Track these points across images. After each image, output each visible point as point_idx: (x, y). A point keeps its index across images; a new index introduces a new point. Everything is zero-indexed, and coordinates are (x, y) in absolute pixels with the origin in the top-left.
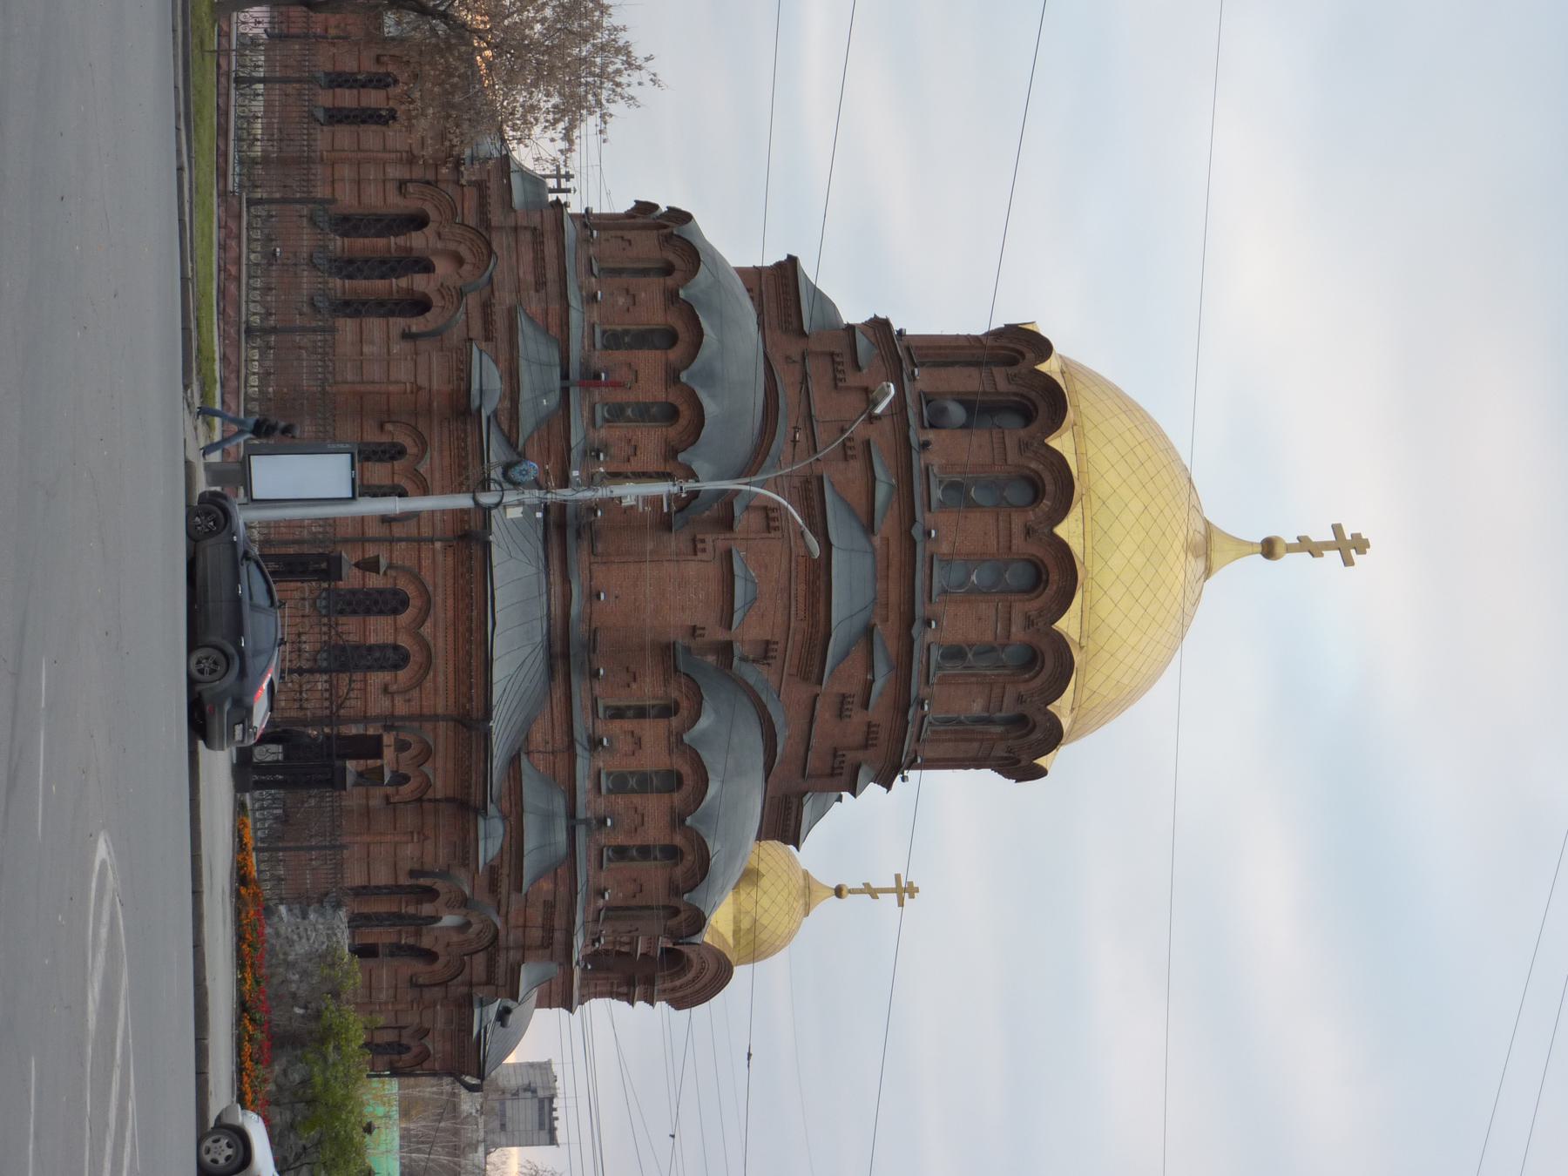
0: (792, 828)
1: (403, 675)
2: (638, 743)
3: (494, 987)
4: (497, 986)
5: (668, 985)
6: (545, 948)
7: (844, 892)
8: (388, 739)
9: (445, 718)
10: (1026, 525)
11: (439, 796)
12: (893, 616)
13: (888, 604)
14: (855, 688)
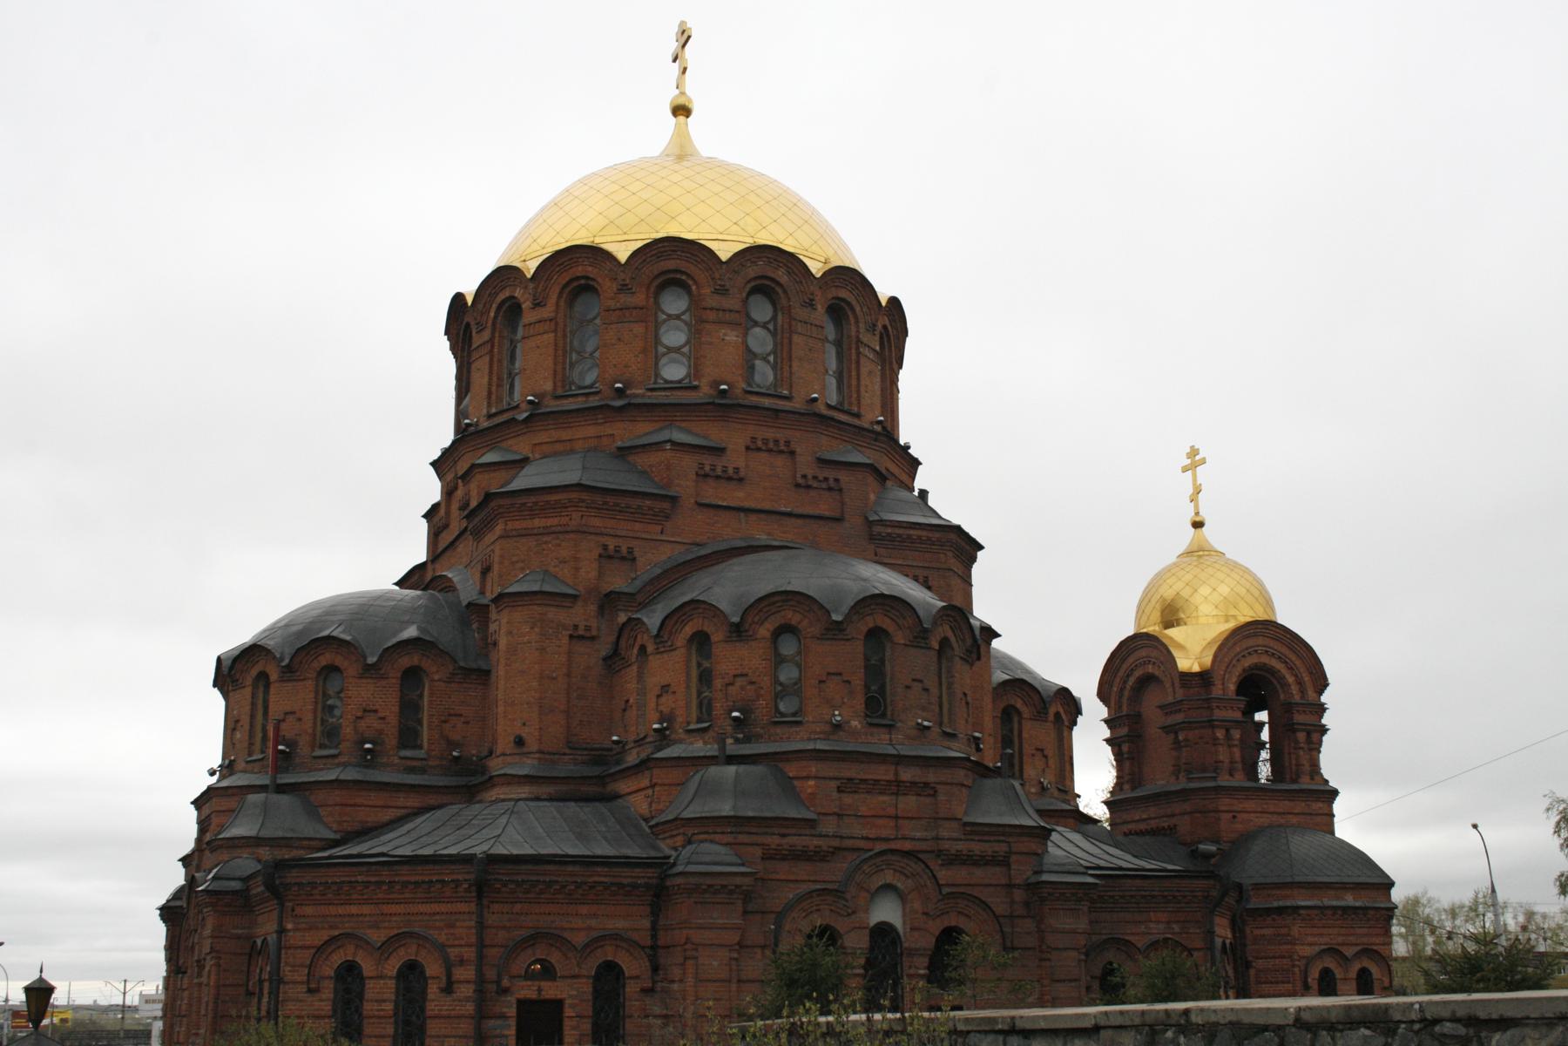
0: (924, 533)
1: (433, 968)
2: (665, 688)
3: (1013, 858)
4: (1010, 852)
5: (1294, 689)
6: (936, 792)
7: (1198, 519)
8: (528, 991)
9: (481, 915)
10: (533, 308)
11: (646, 923)
12: (608, 429)
13: (598, 437)
14: (688, 464)
